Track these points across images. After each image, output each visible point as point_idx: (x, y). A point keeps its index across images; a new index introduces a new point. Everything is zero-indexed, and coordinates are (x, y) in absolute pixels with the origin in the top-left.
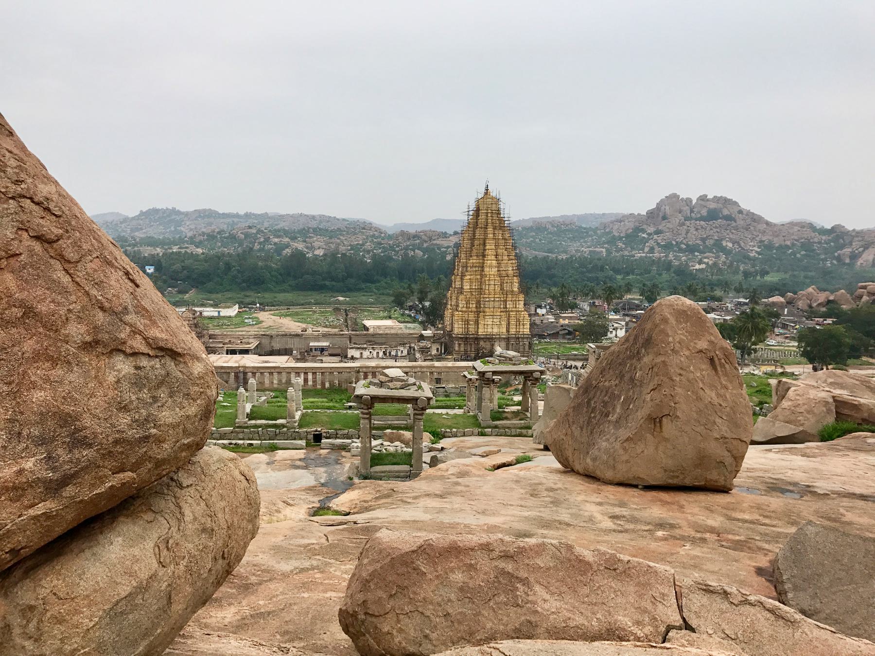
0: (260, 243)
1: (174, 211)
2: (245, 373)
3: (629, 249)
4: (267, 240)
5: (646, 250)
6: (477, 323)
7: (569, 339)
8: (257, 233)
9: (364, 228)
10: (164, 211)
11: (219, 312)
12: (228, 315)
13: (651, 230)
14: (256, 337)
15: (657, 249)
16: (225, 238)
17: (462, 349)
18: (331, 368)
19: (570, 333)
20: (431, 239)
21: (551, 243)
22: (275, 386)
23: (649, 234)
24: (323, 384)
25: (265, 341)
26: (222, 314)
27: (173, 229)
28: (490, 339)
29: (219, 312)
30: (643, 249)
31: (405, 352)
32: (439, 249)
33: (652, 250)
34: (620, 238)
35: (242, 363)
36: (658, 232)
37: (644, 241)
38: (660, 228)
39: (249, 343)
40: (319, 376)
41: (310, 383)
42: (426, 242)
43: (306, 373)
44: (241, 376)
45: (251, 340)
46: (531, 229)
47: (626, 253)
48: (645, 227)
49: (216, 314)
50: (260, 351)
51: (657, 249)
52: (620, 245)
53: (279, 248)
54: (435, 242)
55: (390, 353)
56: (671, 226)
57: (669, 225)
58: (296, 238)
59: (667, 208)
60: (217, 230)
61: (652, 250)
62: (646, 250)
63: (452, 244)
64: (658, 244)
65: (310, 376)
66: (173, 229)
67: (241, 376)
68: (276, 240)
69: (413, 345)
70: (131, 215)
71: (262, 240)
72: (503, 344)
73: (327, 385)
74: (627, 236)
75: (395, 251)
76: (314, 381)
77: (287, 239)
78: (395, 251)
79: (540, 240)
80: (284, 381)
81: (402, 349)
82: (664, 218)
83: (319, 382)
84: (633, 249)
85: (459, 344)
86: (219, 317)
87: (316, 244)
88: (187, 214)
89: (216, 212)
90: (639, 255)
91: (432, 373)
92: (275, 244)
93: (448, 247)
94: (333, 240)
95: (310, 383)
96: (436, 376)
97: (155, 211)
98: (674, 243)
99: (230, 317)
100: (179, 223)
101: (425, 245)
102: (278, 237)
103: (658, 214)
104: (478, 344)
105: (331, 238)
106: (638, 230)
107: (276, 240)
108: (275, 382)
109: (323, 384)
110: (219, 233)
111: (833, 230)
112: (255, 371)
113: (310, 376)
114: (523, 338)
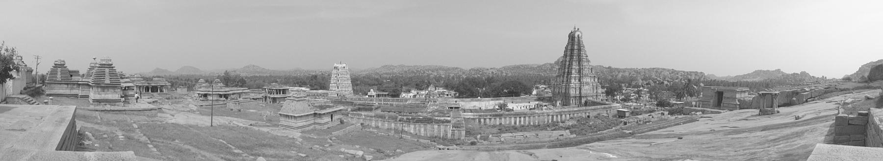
53: (428, 75)
111: (609, 68)
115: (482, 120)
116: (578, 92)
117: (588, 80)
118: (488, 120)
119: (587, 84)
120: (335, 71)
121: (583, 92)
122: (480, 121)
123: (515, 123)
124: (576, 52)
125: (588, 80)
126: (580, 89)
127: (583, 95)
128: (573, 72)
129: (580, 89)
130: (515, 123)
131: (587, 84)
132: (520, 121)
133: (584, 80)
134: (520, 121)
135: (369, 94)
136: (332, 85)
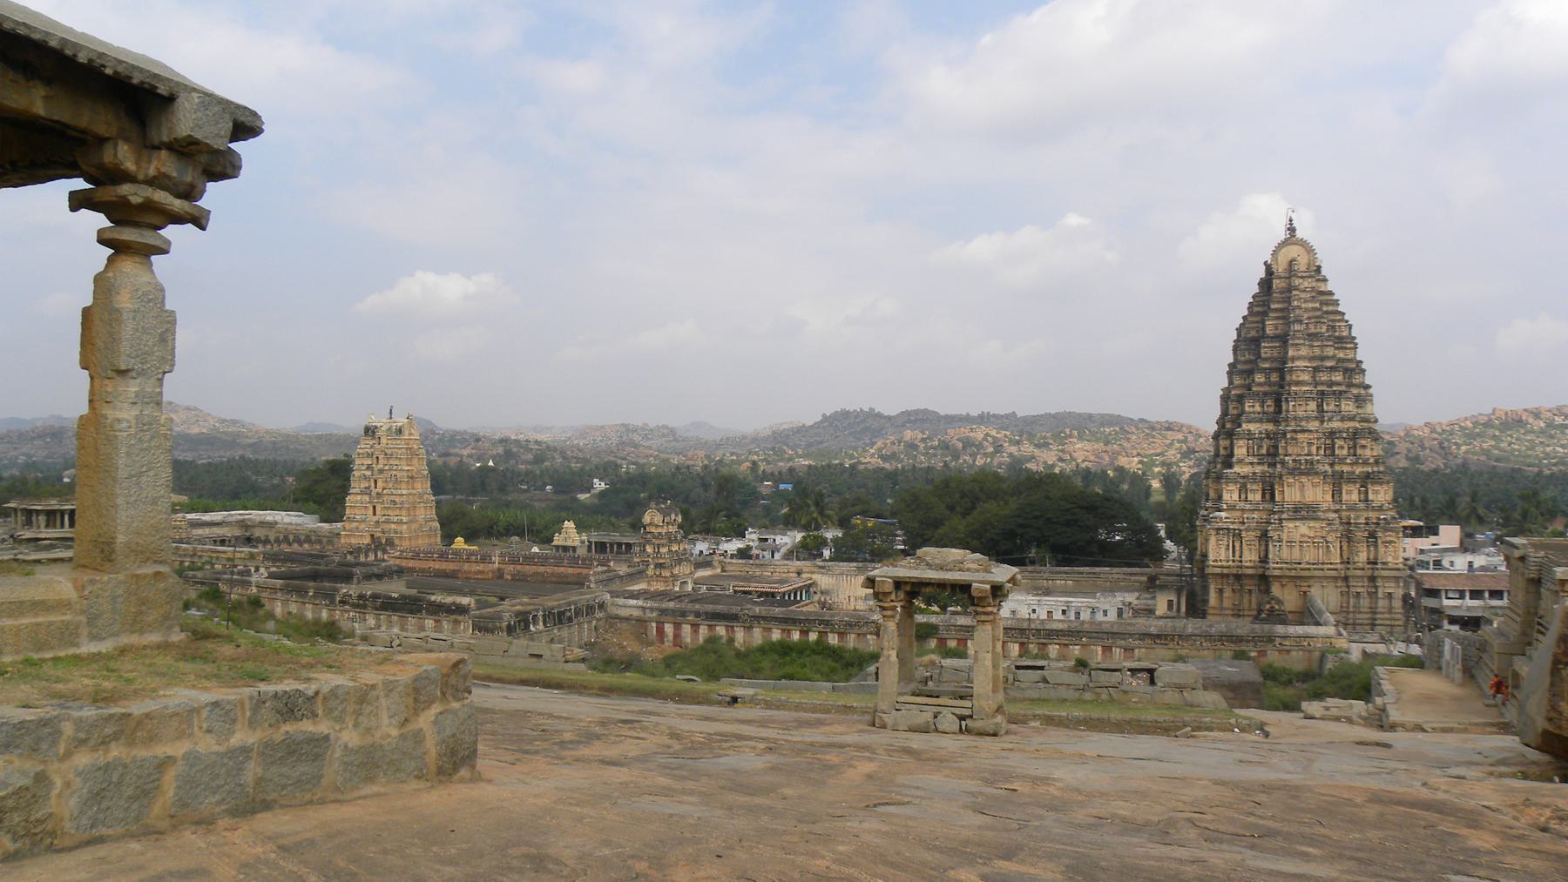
0: (986, 455)
1: (873, 415)
9: (1168, 429)
10: (857, 414)
21: (1532, 448)
28: (1299, 579)
46: (1488, 424)
58: (1046, 445)
60: (920, 436)
68: (1013, 449)
70: (809, 423)
71: (991, 449)
79: (1510, 444)
85: (1221, 591)
88: (889, 418)
92: (1011, 455)
94: (1109, 448)
97: (845, 414)
104: (1267, 591)
107: (1013, 449)
110: (923, 440)
115: (669, 629)
116: (1250, 556)
117: (1316, 493)
118: (687, 629)
119: (1304, 512)
120: (365, 445)
121: (1280, 555)
122: (660, 631)
124: (1267, 349)
125: (1316, 493)
126: (1264, 537)
127: (1274, 569)
128: (1240, 451)
129: (1264, 537)
131: (1304, 512)
133: (1291, 493)
135: (558, 540)
136: (355, 501)
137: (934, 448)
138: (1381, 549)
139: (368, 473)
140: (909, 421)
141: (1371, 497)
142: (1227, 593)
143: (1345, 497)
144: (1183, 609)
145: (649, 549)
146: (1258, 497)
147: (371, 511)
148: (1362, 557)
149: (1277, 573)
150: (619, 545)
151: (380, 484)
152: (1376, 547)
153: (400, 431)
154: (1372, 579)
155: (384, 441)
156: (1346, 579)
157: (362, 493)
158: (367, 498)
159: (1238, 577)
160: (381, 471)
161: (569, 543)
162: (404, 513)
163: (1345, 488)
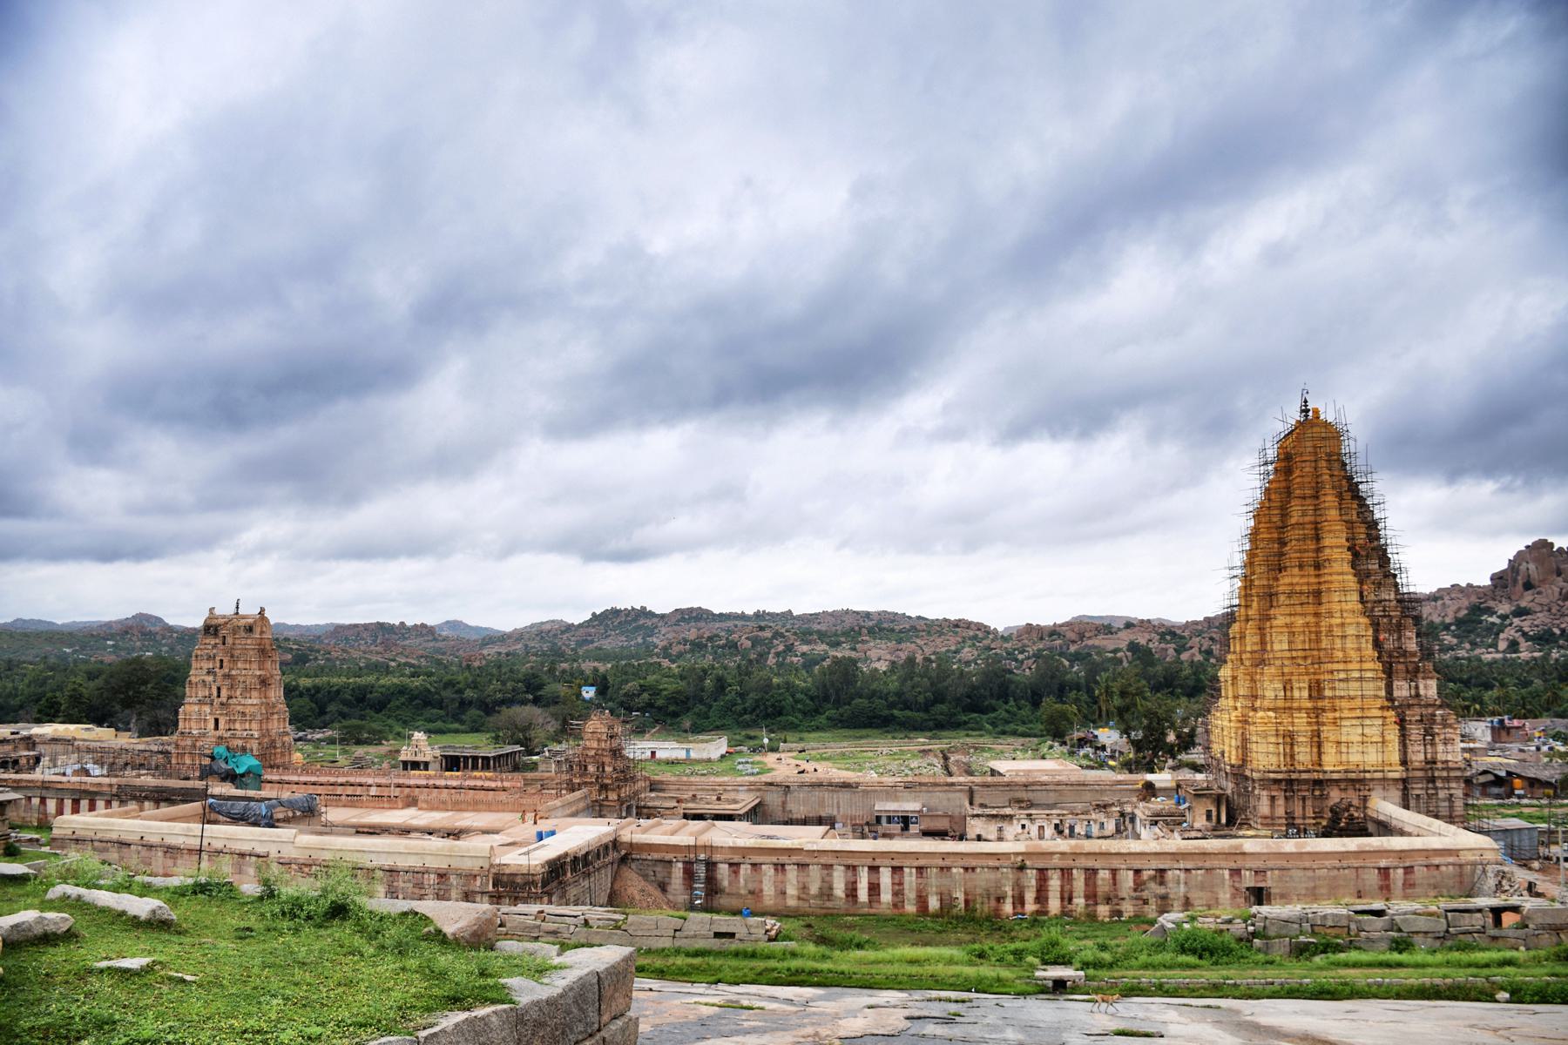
0: (778, 654)
1: (644, 613)
2: (711, 865)
3: (1467, 646)
4: (789, 649)
5: (1502, 645)
6: (1317, 742)
7: (1498, 796)
8: (774, 637)
10: (627, 612)
11: (688, 751)
12: (705, 756)
13: (1504, 608)
14: (752, 787)
15: (1524, 645)
16: (719, 647)
17: (1280, 811)
18: (944, 856)
19: (1499, 781)
20: (1082, 637)
22: (792, 903)
23: (1504, 617)
24: (922, 901)
25: (774, 799)
26: (693, 755)
27: (640, 640)
28: (1358, 782)
29: (688, 751)
30: (1495, 645)
31: (1110, 827)
32: (1098, 654)
33: (1513, 646)
34: (1447, 627)
35: (704, 839)
36: (1521, 612)
37: (1495, 631)
38: (1523, 604)
39: (735, 801)
40: (910, 878)
41: (886, 896)
42: (1074, 642)
43: (874, 869)
44: (701, 871)
45: (741, 796)
47: (1462, 653)
48: (1491, 603)
49: (682, 755)
50: (757, 814)
51: (1524, 645)
52: (1448, 639)
53: (810, 662)
54: (1090, 642)
55: (1072, 828)
56: (1545, 601)
57: (1539, 599)
58: (838, 644)
59: (1532, 566)
61: (1513, 646)
62: (1502, 645)
63: (1123, 645)
64: (1525, 634)
65: (886, 878)
66: (640, 640)
67: (701, 871)
68: (805, 648)
69: (1128, 809)
71: (781, 648)
72: (1396, 794)
73: (934, 904)
74: (1459, 622)
75: (1016, 660)
76: (898, 893)
77: (824, 647)
78: (1016, 660)
80: (814, 889)
81: (1101, 817)
82: (1528, 586)
83: (910, 894)
84: (1474, 645)
85: (1273, 798)
86: (688, 761)
87: (873, 654)
88: (663, 616)
89: (708, 612)
90: (1488, 657)
91: (1236, 872)
92: (803, 654)
93: (1115, 651)
94: (903, 645)
95: (886, 896)
96: (1249, 880)
97: (615, 612)
98: (1557, 631)
99: (709, 760)
100: (651, 631)
101: (1073, 649)
102: (808, 643)
103: (1515, 581)
105: (899, 641)
106: (1477, 610)
107: (805, 648)
108: (792, 891)
109: (922, 901)
110: (710, 639)
112: (736, 859)
113: (886, 878)
114: (1447, 779)
123: (852, 892)
130: (852, 892)
132: (874, 889)
134: (874, 889)
137: (723, 647)
138: (1440, 748)
139: (211, 678)
140: (683, 619)
141: (1422, 692)
142: (1281, 802)
143: (1396, 694)
144: (1224, 820)
145: (591, 769)
146: (1305, 694)
147: (211, 725)
148: (1417, 755)
149: (1335, 776)
150: (475, 758)
151: (224, 693)
152: (1433, 744)
153: (250, 629)
154: (1432, 780)
155: (229, 640)
156: (1404, 781)
157: (200, 703)
158: (207, 709)
159: (1290, 782)
160: (227, 676)
161: (419, 758)
162: (255, 726)
163: (1395, 683)
